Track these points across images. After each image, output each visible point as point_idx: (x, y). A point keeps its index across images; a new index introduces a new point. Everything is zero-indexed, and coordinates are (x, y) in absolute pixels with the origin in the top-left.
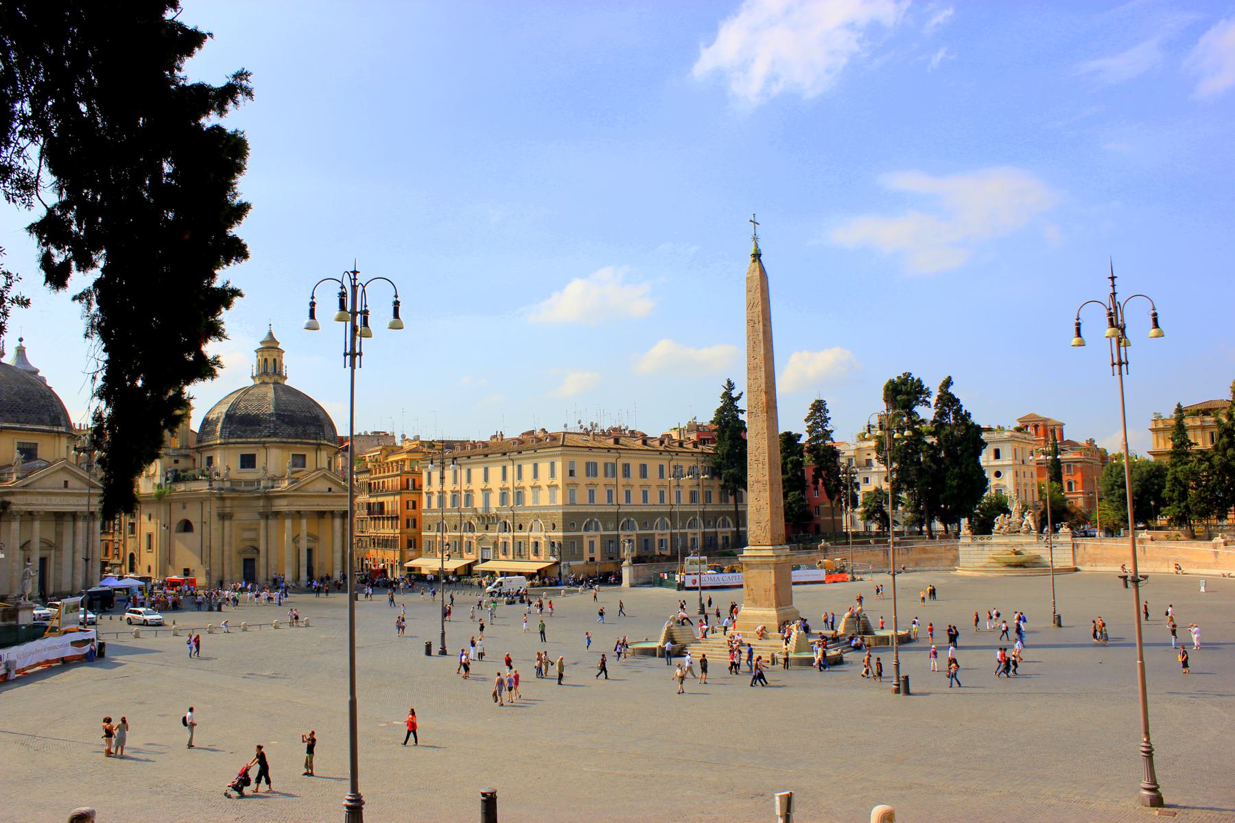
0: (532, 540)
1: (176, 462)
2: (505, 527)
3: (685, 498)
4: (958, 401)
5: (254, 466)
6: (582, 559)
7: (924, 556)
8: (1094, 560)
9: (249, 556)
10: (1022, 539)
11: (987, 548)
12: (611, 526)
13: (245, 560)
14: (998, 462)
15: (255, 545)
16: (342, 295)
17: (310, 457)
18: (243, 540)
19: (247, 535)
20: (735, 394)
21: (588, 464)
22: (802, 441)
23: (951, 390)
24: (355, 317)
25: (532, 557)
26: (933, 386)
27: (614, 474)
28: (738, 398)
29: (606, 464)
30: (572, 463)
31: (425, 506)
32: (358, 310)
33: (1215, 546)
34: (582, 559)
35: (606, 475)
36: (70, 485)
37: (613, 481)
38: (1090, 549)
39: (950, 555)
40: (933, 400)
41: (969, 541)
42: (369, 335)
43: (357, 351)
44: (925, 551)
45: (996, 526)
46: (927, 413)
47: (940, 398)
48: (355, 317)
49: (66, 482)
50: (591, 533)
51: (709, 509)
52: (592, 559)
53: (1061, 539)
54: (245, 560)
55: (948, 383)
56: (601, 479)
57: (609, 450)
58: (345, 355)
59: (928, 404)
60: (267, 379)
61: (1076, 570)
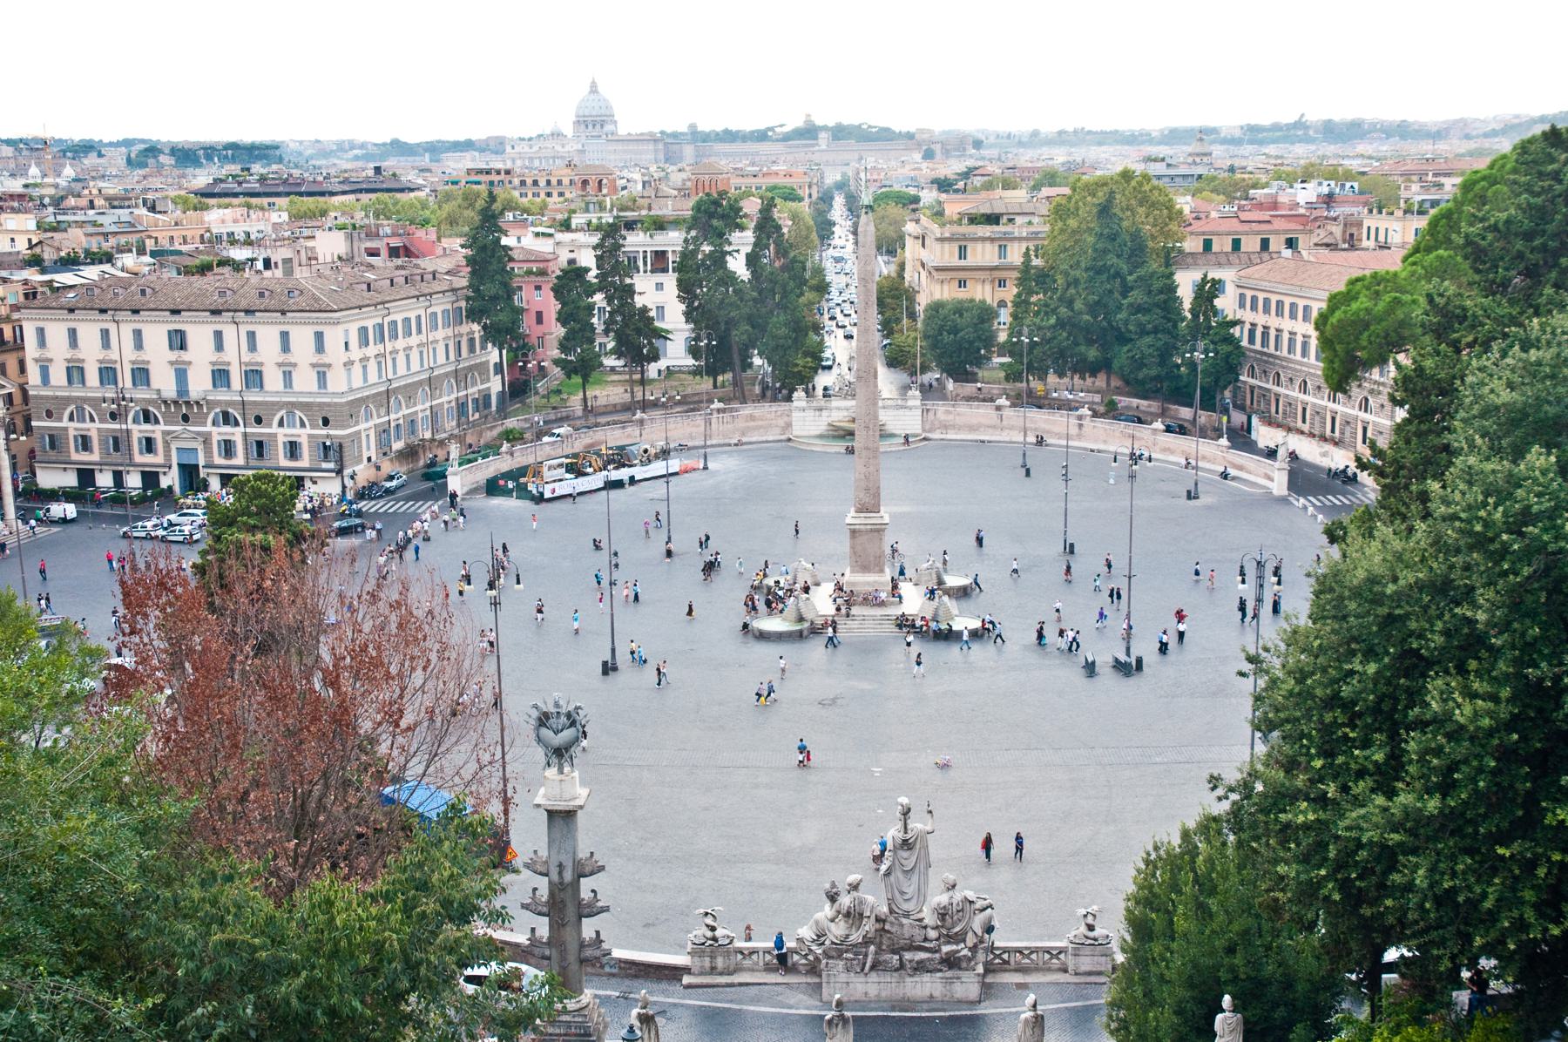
2: (227, 419)
3: (441, 359)
7: (752, 424)
8: (945, 427)
11: (825, 413)
12: (383, 411)
20: (497, 206)
33: (1080, 418)
38: (941, 416)
41: (803, 404)
53: (910, 403)
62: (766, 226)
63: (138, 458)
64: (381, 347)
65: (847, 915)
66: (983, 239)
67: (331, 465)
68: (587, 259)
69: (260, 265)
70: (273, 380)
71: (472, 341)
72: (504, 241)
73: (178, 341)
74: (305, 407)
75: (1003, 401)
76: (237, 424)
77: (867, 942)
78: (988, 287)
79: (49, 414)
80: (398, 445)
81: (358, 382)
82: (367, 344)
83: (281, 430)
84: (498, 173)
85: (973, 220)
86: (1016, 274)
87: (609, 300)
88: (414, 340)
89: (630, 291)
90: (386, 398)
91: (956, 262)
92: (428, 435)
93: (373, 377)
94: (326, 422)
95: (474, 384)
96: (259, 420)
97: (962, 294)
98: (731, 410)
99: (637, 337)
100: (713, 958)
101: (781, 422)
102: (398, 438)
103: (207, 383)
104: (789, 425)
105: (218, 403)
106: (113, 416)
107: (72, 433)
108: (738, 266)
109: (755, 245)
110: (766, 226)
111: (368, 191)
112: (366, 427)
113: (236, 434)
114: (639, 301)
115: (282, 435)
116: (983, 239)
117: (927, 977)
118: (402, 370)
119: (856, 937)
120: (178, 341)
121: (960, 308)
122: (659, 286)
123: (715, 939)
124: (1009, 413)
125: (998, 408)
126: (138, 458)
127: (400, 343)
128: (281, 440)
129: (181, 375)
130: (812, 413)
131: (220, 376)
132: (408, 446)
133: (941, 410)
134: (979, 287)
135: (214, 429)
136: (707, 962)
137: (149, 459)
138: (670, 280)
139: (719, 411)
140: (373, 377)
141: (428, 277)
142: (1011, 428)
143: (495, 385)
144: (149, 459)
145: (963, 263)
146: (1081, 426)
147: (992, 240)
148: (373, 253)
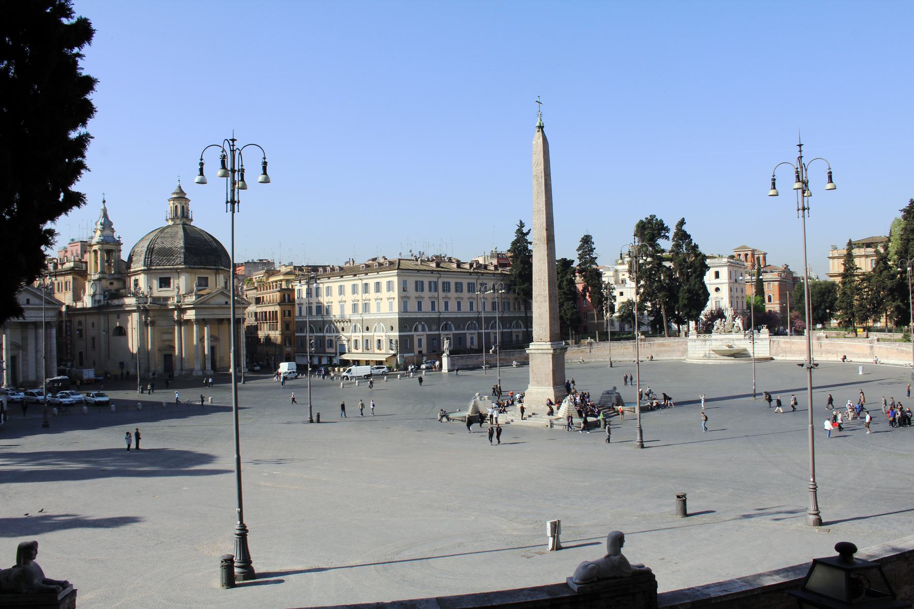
0: (376, 338)
1: (111, 284)
3: (489, 307)
4: (689, 236)
5: (169, 286)
6: (412, 351)
7: (663, 349)
9: (167, 352)
10: (733, 336)
11: (708, 343)
12: (434, 327)
13: (165, 356)
14: (717, 281)
15: (171, 344)
16: (224, 158)
17: (211, 280)
18: (164, 341)
19: (167, 337)
20: (525, 230)
21: (416, 282)
22: (575, 265)
23: (684, 228)
24: (233, 172)
25: (377, 351)
26: (671, 224)
27: (436, 290)
28: (527, 233)
29: (430, 283)
30: (405, 283)
31: (297, 314)
32: (236, 168)
33: (871, 342)
34: (412, 351)
35: (430, 290)
36: (31, 302)
37: (436, 294)
38: (782, 345)
39: (681, 348)
40: (671, 235)
42: (244, 187)
43: (236, 199)
44: (663, 345)
45: (715, 328)
46: (666, 245)
47: (676, 235)
48: (233, 172)
49: (28, 300)
50: (420, 333)
51: (506, 315)
52: (420, 352)
53: (762, 336)
54: (165, 356)
55: (682, 222)
56: (426, 294)
57: (432, 271)
58: (227, 202)
59: (667, 238)
60: (178, 222)
61: (772, 359)
101: (681, 348)
125: (819, 338)
130: (699, 343)
139: (641, 340)
146: (871, 347)
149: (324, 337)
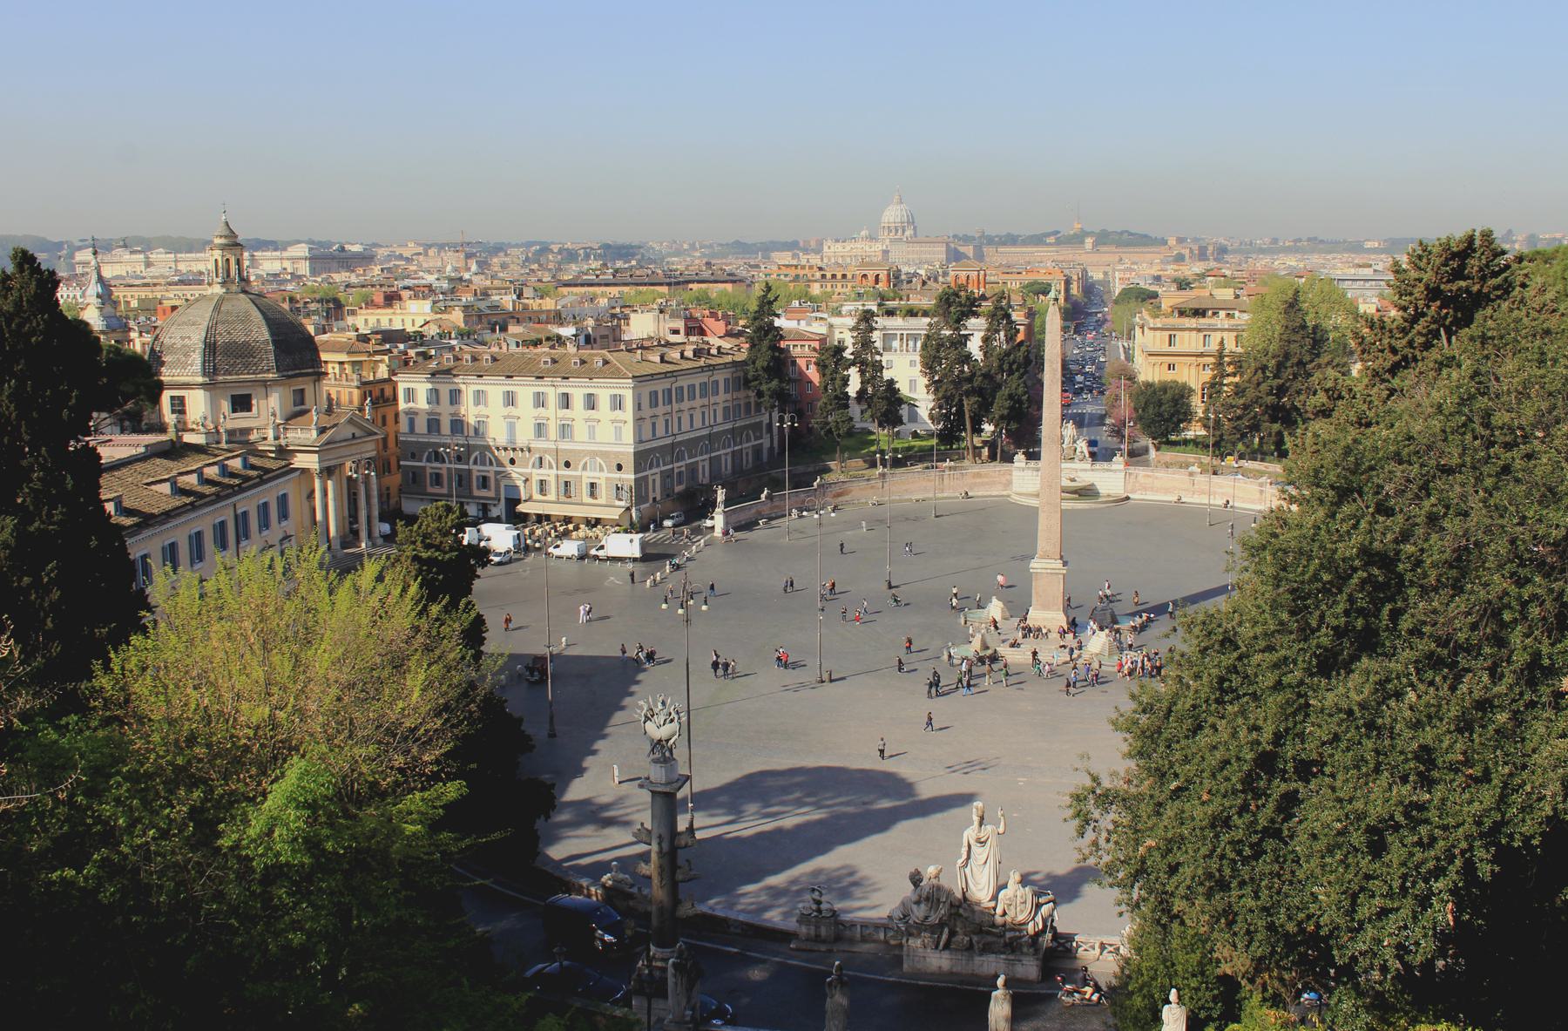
3: (720, 419)
12: (668, 458)
33: (1261, 485)
38: (1141, 479)
39: (1003, 480)
44: (978, 475)
50: (655, 470)
53: (1114, 467)
62: (1000, 315)
63: (476, 493)
64: (668, 408)
65: (927, 899)
66: (1191, 330)
67: (622, 503)
68: (849, 342)
69: (582, 338)
70: (580, 431)
71: (748, 405)
72: (777, 323)
73: (510, 399)
74: (604, 455)
75: (1195, 469)
76: (551, 467)
77: (941, 925)
78: (1193, 370)
79: (413, 456)
80: (678, 489)
81: (647, 434)
82: (657, 405)
83: (585, 474)
84: (803, 267)
85: (1182, 313)
86: (1212, 360)
87: (862, 372)
88: (698, 402)
89: (879, 367)
90: (673, 451)
91: (1166, 348)
92: (706, 481)
93: (660, 431)
94: (620, 467)
95: (748, 440)
96: (567, 465)
97: (1169, 376)
98: (962, 468)
99: (889, 404)
100: (817, 927)
102: (680, 483)
103: (531, 433)
104: (1009, 483)
105: (538, 449)
106: (459, 459)
107: (429, 471)
108: (974, 347)
109: (988, 330)
110: (1000, 315)
111: (699, 282)
112: (654, 474)
113: (549, 474)
114: (887, 375)
115: (587, 477)
116: (1191, 330)
117: (992, 957)
118: (685, 426)
119: (934, 919)
120: (510, 399)
121: (1164, 388)
122: (912, 363)
123: (819, 911)
124: (1200, 478)
125: (1191, 474)
126: (476, 493)
127: (686, 405)
128: (586, 482)
129: (512, 429)
131: (540, 429)
132: (687, 489)
133: (1140, 472)
134: (1186, 371)
135: (535, 471)
136: (812, 932)
137: (484, 493)
138: (918, 359)
140: (660, 431)
141: (714, 351)
142: (1202, 492)
143: (765, 442)
144: (484, 493)
145: (1172, 349)
147: (1199, 330)
148: (676, 332)
149: (470, 471)
